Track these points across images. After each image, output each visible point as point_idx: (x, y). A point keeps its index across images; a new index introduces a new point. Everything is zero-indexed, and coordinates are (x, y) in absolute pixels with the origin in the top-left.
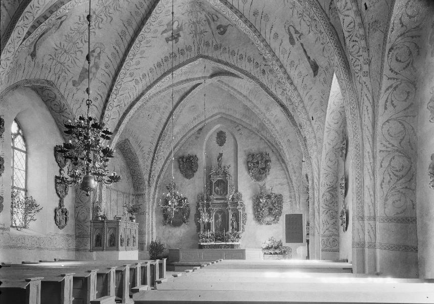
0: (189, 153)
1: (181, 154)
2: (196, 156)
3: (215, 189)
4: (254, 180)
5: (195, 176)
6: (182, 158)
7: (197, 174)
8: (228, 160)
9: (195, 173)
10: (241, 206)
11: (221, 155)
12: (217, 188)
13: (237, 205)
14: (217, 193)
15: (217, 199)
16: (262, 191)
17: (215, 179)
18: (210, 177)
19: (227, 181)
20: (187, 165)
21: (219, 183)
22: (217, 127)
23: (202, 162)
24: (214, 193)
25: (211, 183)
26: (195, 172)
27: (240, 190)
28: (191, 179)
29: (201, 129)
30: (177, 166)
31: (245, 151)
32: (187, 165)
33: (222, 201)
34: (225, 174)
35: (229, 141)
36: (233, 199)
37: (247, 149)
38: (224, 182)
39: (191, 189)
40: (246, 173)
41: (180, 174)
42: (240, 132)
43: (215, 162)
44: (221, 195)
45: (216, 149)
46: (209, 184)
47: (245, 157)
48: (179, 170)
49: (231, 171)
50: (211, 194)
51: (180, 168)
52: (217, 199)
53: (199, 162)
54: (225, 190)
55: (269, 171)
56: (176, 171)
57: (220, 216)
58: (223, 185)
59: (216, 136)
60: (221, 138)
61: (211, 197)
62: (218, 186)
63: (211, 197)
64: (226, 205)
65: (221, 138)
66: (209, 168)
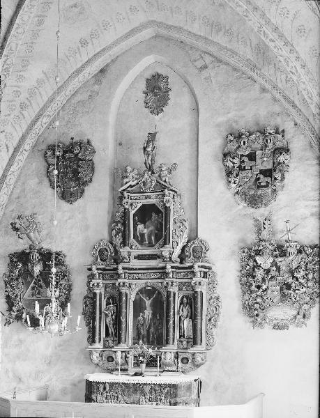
0: (72, 135)
1: (52, 139)
2: (89, 142)
4: (243, 204)
5: (86, 193)
6: (52, 148)
7: (89, 190)
8: (172, 150)
9: (86, 188)
10: (205, 275)
11: (152, 137)
12: (140, 227)
14: (141, 239)
15: (139, 257)
16: (265, 234)
17: (135, 204)
18: (121, 198)
19: (167, 209)
20: (69, 166)
21: (145, 213)
22: (146, 65)
23: (104, 157)
24: (132, 240)
25: (126, 214)
26: (85, 183)
27: (201, 235)
28: (76, 204)
29: (102, 71)
30: (43, 171)
31: (218, 125)
32: (69, 166)
33: (153, 263)
34: (161, 188)
35: (178, 100)
36: (182, 258)
37: (221, 119)
38: (158, 211)
39: (75, 230)
40: (220, 184)
41: (50, 190)
42: (205, 73)
43: (139, 158)
44: (151, 245)
45: (141, 123)
46: (120, 224)
47: (219, 142)
48: (46, 180)
49: (180, 180)
50: (124, 243)
51: (48, 173)
52: (139, 257)
53: (96, 159)
54: (161, 235)
55: (283, 178)
56: (40, 182)
57: (148, 303)
58: (155, 218)
59: (142, 86)
60: (157, 92)
62: (143, 222)
63: (124, 251)
64: (163, 273)
65: (157, 92)
66: (119, 174)
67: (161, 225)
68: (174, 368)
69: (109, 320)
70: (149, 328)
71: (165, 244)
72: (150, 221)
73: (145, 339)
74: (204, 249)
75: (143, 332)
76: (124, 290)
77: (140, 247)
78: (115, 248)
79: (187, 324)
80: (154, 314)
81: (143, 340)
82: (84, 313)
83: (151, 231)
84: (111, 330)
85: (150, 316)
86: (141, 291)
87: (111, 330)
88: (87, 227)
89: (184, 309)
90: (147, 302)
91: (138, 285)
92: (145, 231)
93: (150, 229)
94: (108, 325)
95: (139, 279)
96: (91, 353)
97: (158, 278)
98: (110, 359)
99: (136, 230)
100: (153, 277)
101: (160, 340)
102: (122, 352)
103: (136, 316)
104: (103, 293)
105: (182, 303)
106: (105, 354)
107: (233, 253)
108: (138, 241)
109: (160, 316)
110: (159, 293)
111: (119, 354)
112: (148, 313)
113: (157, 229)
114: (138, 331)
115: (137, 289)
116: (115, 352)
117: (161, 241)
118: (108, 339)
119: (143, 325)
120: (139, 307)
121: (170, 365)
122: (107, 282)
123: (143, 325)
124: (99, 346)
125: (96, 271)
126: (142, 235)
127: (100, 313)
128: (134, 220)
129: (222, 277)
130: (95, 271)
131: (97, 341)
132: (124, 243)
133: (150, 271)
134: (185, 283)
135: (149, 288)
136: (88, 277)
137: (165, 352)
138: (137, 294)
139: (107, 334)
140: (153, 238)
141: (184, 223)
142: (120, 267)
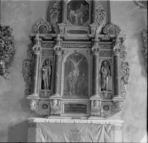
3: (68, 14)
12: (72, 12)
13: (114, 44)
15: (71, 32)
27: (114, 21)
33: (83, 36)
57: (76, 65)
61: (62, 26)
62: (74, 9)
67: (88, 12)
68: (99, 114)
69: (45, 76)
70: (77, 83)
71: (92, 22)
72: (79, 9)
73: (74, 92)
74: (117, 30)
75: (72, 85)
76: (59, 54)
77: (72, 25)
78: (52, 26)
79: (108, 81)
80: (81, 73)
81: (72, 92)
82: (23, 72)
83: (80, 15)
84: (46, 84)
85: (78, 74)
86: (70, 56)
87: (46, 84)
88: (30, 13)
89: (105, 70)
90: (75, 64)
91: (70, 51)
92: (76, 15)
93: (80, 14)
94: (44, 80)
95: (69, 47)
96: (30, 101)
97: (85, 47)
98: (45, 107)
99: (69, 14)
100: (80, 47)
101: (86, 91)
102: (58, 100)
103: (66, 74)
104: (41, 57)
105: (103, 65)
106: (42, 102)
107: (136, 35)
108: (70, 21)
109: (85, 74)
110: (85, 58)
111: (56, 102)
112: (76, 72)
113: (84, 14)
114: (68, 86)
115: (68, 55)
116: (52, 100)
117: (88, 22)
118: (44, 90)
119: (72, 81)
120: (69, 68)
121: (96, 111)
122: (46, 48)
123: (72, 81)
124: (36, 95)
125: (39, 38)
126: (74, 18)
127: (39, 71)
128: (68, 8)
129: (129, 50)
130: (37, 38)
131: (36, 92)
132: (60, 21)
133: (78, 42)
134: (105, 51)
135: (77, 55)
136: (29, 45)
137: (94, 101)
138: (68, 58)
139: (43, 88)
140: (81, 20)
141: (103, 12)
142: (59, 35)
